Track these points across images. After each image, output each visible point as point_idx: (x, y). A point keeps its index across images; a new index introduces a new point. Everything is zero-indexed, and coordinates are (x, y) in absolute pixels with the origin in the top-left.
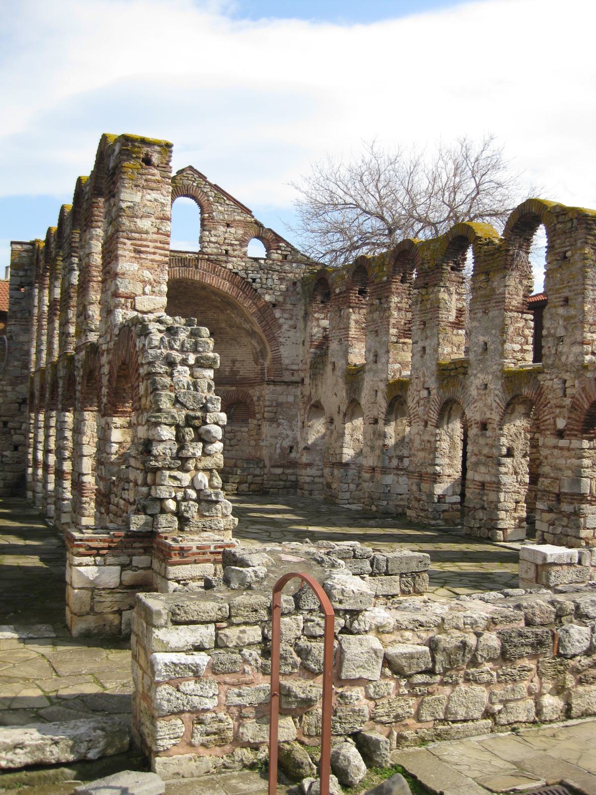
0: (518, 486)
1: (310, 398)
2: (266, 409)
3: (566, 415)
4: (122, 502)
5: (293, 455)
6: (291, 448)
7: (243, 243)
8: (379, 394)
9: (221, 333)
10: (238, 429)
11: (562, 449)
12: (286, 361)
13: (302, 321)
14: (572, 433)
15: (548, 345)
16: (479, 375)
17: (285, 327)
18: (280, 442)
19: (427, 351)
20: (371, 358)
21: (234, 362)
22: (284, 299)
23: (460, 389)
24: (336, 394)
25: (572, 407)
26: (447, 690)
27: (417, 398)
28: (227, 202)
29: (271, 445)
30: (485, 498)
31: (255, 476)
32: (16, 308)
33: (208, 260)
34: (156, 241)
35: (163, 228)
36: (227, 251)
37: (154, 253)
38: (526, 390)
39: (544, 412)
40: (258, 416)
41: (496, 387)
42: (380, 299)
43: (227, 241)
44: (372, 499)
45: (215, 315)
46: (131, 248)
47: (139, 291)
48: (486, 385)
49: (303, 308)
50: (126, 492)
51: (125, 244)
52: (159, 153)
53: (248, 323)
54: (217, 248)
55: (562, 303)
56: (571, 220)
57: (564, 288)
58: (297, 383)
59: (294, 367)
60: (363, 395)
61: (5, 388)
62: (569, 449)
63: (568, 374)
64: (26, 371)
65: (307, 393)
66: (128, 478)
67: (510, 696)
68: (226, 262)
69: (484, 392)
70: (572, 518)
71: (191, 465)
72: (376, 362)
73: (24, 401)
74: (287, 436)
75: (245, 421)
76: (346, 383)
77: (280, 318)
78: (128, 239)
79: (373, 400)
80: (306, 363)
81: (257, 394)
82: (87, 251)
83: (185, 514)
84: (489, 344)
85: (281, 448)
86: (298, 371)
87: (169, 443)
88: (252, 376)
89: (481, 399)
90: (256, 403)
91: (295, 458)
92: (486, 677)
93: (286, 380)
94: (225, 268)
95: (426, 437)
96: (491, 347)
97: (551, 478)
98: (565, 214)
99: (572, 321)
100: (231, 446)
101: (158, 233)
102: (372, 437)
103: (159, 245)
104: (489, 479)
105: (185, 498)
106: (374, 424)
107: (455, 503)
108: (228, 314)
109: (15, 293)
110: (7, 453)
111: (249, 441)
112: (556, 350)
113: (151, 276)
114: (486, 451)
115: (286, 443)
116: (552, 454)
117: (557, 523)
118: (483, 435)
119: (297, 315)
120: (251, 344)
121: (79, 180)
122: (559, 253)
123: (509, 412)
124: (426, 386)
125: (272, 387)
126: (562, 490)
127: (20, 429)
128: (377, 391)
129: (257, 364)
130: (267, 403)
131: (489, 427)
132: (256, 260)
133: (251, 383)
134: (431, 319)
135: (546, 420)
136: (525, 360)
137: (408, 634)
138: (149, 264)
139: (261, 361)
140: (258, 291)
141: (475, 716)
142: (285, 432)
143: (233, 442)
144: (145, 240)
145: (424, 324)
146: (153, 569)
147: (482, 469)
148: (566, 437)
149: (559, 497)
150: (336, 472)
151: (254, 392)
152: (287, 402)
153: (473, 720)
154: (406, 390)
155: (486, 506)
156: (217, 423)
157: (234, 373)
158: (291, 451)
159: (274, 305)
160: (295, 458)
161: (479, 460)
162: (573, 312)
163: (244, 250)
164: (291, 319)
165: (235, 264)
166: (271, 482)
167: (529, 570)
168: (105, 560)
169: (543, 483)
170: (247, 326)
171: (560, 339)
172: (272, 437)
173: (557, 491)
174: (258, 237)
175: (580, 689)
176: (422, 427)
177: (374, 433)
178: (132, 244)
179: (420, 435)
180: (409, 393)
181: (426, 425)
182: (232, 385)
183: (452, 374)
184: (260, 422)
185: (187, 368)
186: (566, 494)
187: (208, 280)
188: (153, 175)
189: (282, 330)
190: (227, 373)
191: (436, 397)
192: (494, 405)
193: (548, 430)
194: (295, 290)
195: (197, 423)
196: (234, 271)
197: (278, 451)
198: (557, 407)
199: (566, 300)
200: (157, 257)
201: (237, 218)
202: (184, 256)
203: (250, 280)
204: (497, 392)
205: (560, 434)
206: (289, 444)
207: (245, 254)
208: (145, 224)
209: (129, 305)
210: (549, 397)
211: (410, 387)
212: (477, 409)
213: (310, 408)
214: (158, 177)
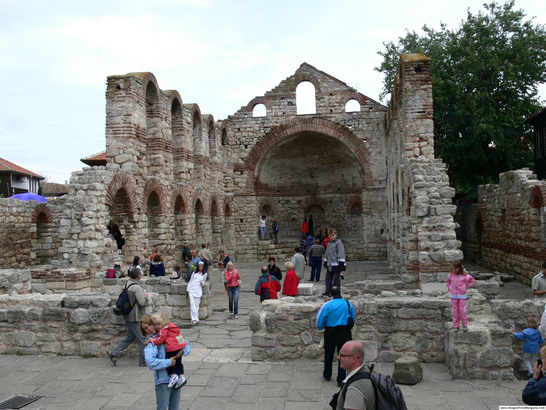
5: (383, 235)
6: (382, 231)
7: (343, 103)
12: (375, 176)
17: (373, 154)
21: (353, 178)
22: (371, 136)
26: (16, 331)
28: (330, 80)
29: (368, 229)
31: (358, 249)
33: (319, 118)
36: (331, 111)
37: (123, 133)
47: (116, 153)
52: (124, 82)
54: (326, 110)
59: (381, 178)
67: (46, 339)
68: (331, 117)
71: (75, 236)
74: (379, 223)
77: (369, 148)
83: (71, 260)
85: (375, 230)
86: (383, 181)
88: (361, 186)
91: (385, 237)
92: (34, 328)
93: (376, 187)
94: (330, 121)
100: (355, 231)
103: (125, 129)
105: (73, 252)
113: (122, 145)
115: (379, 228)
132: (351, 113)
137: (4, 305)
138: (121, 139)
139: (362, 176)
141: (29, 345)
144: (118, 127)
152: (377, 202)
153: (28, 347)
156: (87, 217)
157: (354, 185)
160: (385, 237)
163: (342, 108)
164: (377, 148)
165: (336, 117)
166: (370, 253)
170: (351, 155)
172: (368, 224)
174: (353, 99)
175: (85, 342)
182: (353, 193)
185: (83, 192)
187: (320, 131)
188: (121, 94)
189: (371, 155)
194: (378, 129)
195: (78, 217)
196: (336, 122)
197: (373, 233)
200: (125, 135)
201: (336, 89)
202: (304, 117)
203: (347, 127)
206: (380, 228)
207: (343, 111)
208: (119, 119)
209: (113, 160)
214: (124, 95)
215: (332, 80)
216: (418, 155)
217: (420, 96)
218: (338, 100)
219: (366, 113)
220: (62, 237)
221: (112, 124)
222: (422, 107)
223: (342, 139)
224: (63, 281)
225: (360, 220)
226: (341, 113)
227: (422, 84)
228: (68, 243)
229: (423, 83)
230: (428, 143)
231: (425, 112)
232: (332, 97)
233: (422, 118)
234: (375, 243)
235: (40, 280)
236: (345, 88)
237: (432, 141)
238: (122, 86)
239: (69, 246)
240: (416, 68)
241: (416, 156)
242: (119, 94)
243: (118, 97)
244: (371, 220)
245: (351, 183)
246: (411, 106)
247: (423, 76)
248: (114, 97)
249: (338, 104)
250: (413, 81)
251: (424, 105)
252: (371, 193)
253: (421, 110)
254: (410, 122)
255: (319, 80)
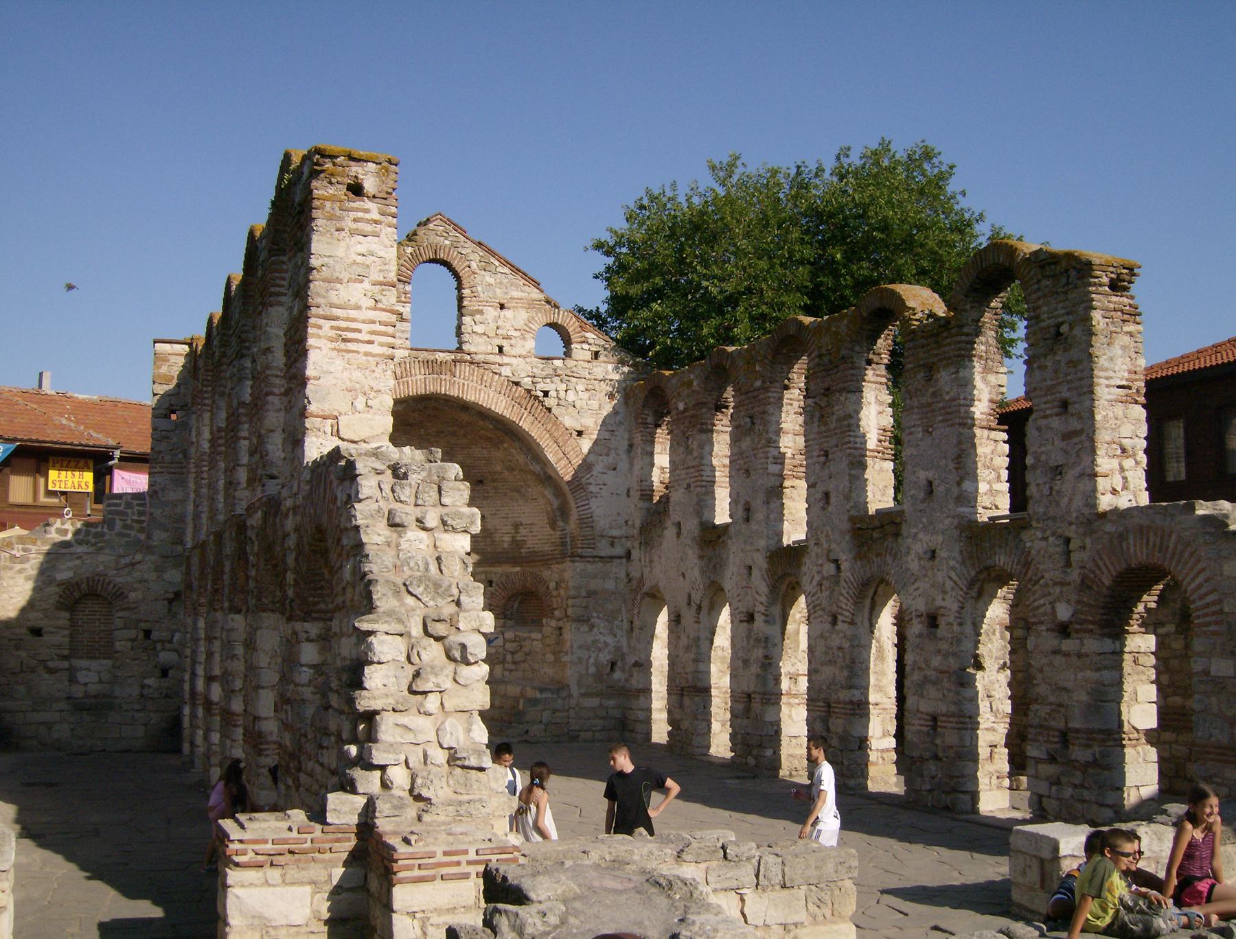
0: (993, 719)
1: (641, 581)
2: (570, 602)
3: (1074, 597)
4: (318, 769)
5: (617, 675)
6: (613, 664)
8: (755, 572)
9: (494, 481)
10: (526, 635)
11: (1067, 654)
12: (602, 523)
13: (624, 457)
14: (1085, 626)
15: (1036, 482)
16: (921, 536)
17: (598, 469)
18: (593, 655)
19: (833, 500)
20: (740, 512)
21: (517, 526)
23: (889, 559)
24: (684, 575)
25: (1083, 581)
27: (817, 578)
28: (500, 269)
30: (938, 741)
32: (163, 446)
33: (472, 363)
34: (374, 322)
35: (384, 299)
36: (501, 349)
37: (370, 342)
38: (1002, 558)
39: (1034, 593)
40: (556, 613)
41: (950, 555)
42: (751, 417)
43: (500, 332)
44: (748, 746)
45: (485, 452)
46: (333, 333)
48: (934, 552)
49: (627, 436)
50: (325, 751)
51: (320, 327)
53: (538, 463)
55: (1056, 410)
56: (1067, 271)
57: (1060, 384)
58: (620, 557)
59: (615, 533)
60: (728, 574)
61: (146, 576)
62: (1080, 655)
63: (1073, 527)
64: (180, 548)
65: (635, 574)
66: (326, 728)
69: (931, 563)
70: (1091, 771)
71: (432, 703)
72: (747, 520)
73: (177, 595)
75: (537, 623)
76: (701, 557)
78: (326, 318)
79: (744, 584)
80: (633, 526)
81: (556, 576)
82: (263, 345)
84: (936, 483)
85: (595, 665)
86: (620, 538)
87: (391, 666)
88: (547, 548)
89: (925, 575)
90: (555, 593)
93: (603, 554)
95: (836, 641)
96: (940, 490)
97: (1051, 704)
98: (1055, 263)
99: (1076, 440)
100: (515, 663)
101: (375, 309)
102: (745, 644)
104: (944, 709)
106: (748, 622)
107: (888, 750)
108: (505, 449)
109: (163, 424)
110: (148, 681)
111: (544, 655)
112: (1051, 488)
114: (936, 661)
115: (605, 657)
116: (1051, 664)
117: (1064, 780)
118: (932, 636)
119: (616, 449)
120: (544, 496)
121: (251, 234)
122: (1049, 327)
123: (974, 595)
124: (832, 557)
125: (580, 566)
126: (1070, 725)
127: (170, 641)
128: (750, 568)
129: (554, 529)
130: (572, 593)
131: (942, 621)
133: (545, 560)
134: (837, 446)
135: (1038, 607)
136: (997, 508)
139: (560, 523)
140: (553, 411)
142: (602, 638)
143: (519, 657)
144: (354, 320)
145: (826, 455)
146: (368, 891)
147: (932, 691)
148: (1074, 635)
149: (1065, 737)
150: (687, 701)
151: (550, 575)
154: (799, 566)
155: (940, 755)
157: (517, 544)
158: (612, 669)
159: (580, 433)
160: (620, 680)
161: (925, 677)
162: (1075, 425)
164: (607, 455)
167: (1028, 870)
168: (283, 876)
169: (1039, 712)
171: (1058, 471)
172: (580, 647)
173: (1062, 725)
176: (828, 626)
177: (749, 637)
178: (332, 328)
179: (826, 639)
180: (804, 569)
181: (834, 622)
183: (876, 533)
184: (561, 624)
186: (1077, 731)
187: (471, 397)
188: (367, 211)
190: (506, 545)
191: (849, 574)
192: (949, 584)
193: (1042, 623)
197: (592, 670)
198: (1055, 584)
199: (1065, 405)
200: (374, 349)
201: (516, 294)
204: (952, 563)
205: (1064, 630)
209: (329, 430)
210: (1041, 567)
211: (806, 560)
212: (918, 593)
213: (642, 598)
214: (375, 215)
215: (506, 270)
216: (1119, 489)
217: (1124, 348)
218: (520, 324)
219: (586, 365)
220: (375, 705)
221: (332, 306)
222: (1126, 375)
223: (526, 424)
224: (466, 876)
225: (535, 635)
226: (525, 357)
227: (1124, 321)
228: (406, 727)
229: (1126, 317)
230: (1137, 463)
231: (1129, 388)
232: (505, 312)
233: (1126, 402)
234: (596, 695)
235: (274, 874)
236: (536, 294)
237: (1143, 458)
238: (370, 185)
239: (410, 737)
240: (1111, 280)
241: (1114, 492)
242: (358, 210)
243: (355, 220)
244: (589, 639)
245: (507, 538)
246: (1107, 370)
247: (1125, 300)
248: (340, 219)
249: (517, 334)
250: (1107, 310)
251: (1130, 372)
252: (590, 567)
253: (1124, 383)
254: (1105, 409)
255: (474, 265)
